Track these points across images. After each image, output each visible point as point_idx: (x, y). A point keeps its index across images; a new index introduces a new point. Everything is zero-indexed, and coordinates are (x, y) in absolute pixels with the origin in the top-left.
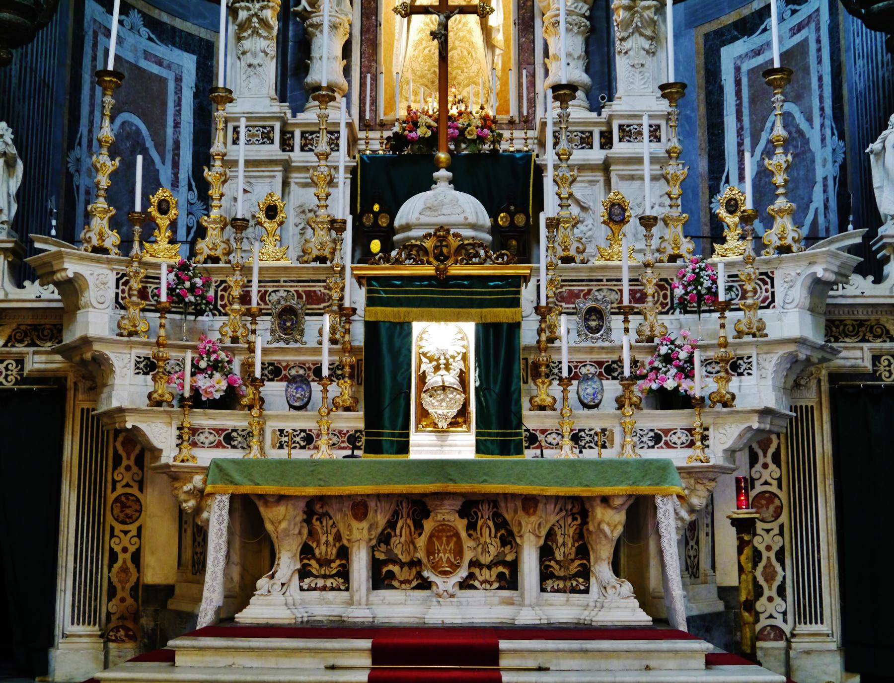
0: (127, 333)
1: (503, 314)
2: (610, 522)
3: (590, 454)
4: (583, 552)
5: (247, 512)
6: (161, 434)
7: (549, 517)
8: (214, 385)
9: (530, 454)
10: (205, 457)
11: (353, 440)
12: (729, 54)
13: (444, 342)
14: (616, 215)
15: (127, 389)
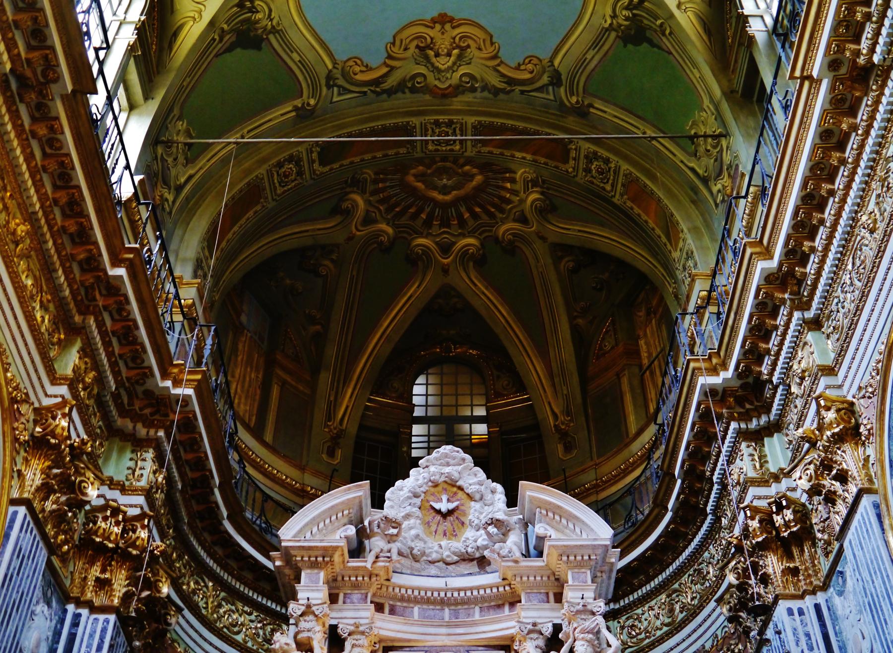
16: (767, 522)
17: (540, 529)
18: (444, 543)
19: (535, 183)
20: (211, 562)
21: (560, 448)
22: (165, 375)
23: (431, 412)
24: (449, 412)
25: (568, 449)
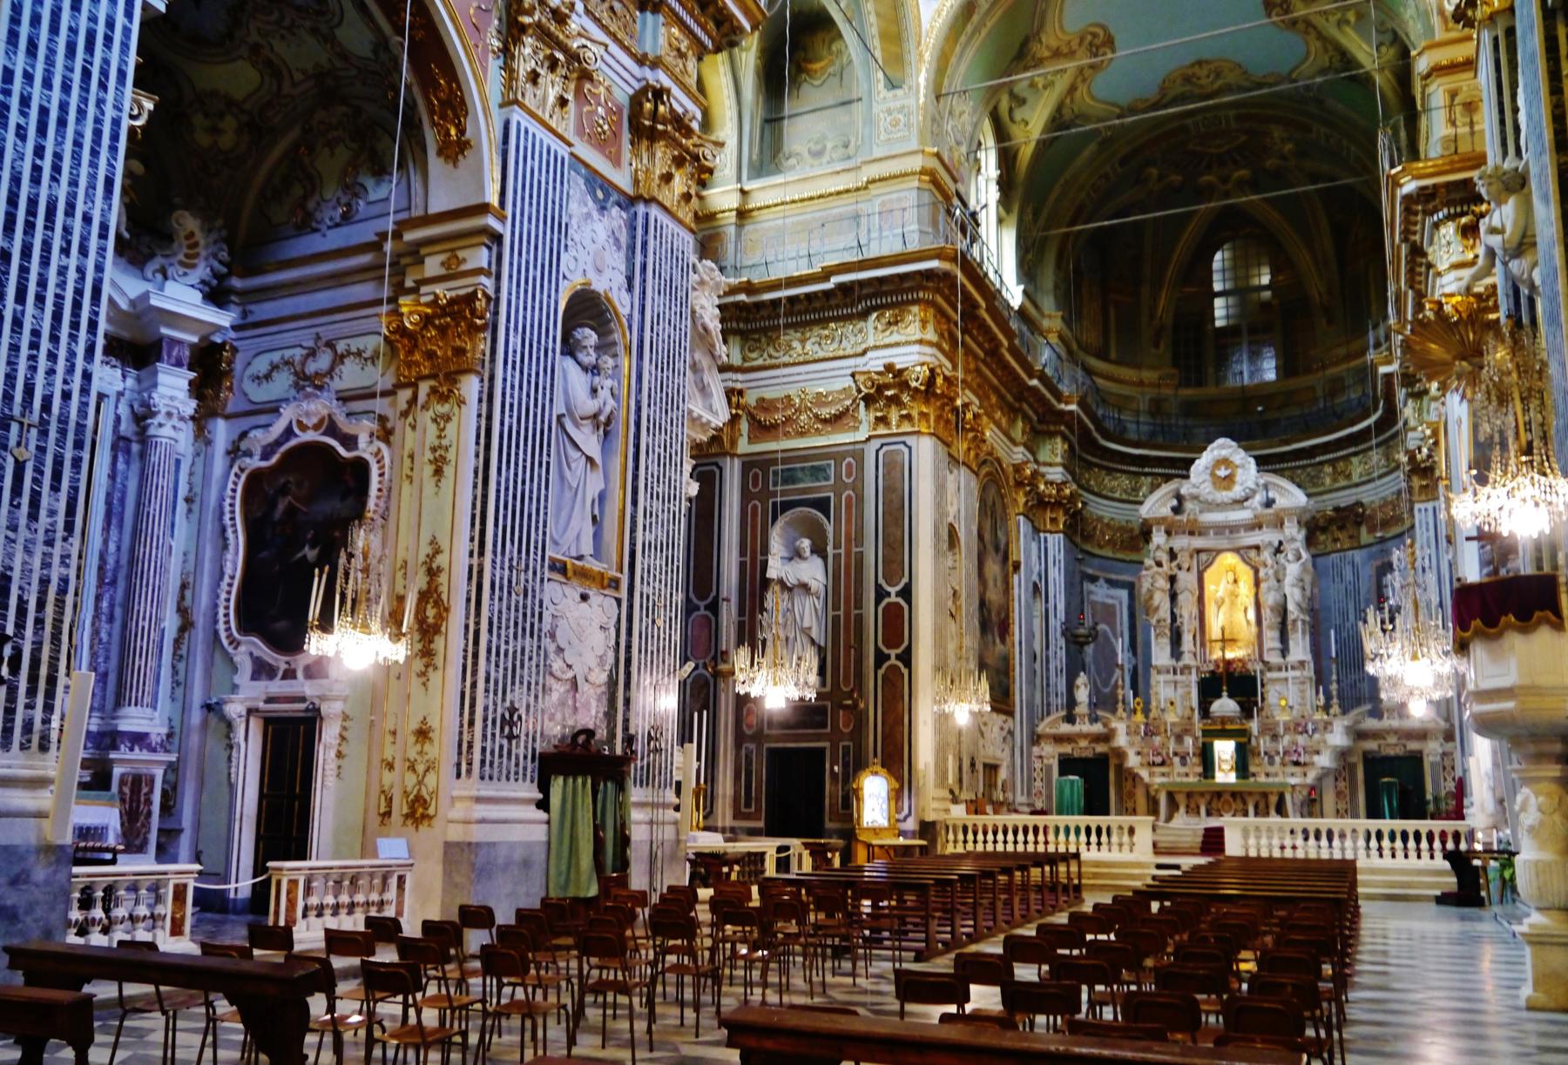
0: (1132, 744)
1: (1244, 740)
2: (1273, 800)
3: (1271, 780)
5: (1171, 796)
6: (1144, 774)
7: (1257, 798)
8: (1158, 760)
9: (1252, 779)
13: (1224, 749)
15: (1133, 761)
16: (1412, 458)
17: (1271, 495)
18: (1224, 493)
20: (1095, 460)
23: (1229, 286)
24: (1241, 284)
25: (1330, 322)
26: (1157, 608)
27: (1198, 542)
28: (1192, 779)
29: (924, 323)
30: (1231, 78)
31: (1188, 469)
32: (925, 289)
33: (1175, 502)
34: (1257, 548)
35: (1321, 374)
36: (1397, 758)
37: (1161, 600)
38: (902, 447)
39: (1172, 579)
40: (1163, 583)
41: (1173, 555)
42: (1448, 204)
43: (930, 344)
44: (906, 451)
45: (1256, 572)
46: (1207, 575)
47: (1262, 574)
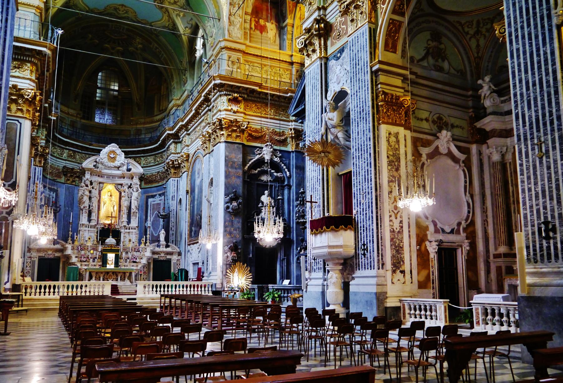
2: (128, 274)
4: (125, 277)
7: (122, 274)
8: (85, 259)
10: (86, 267)
11: (100, 265)
12: (150, 200)
13: (111, 257)
14: (130, 241)
15: (74, 260)
16: (173, 163)
19: (141, 44)
21: (137, 109)
22: (50, 115)
23: (103, 86)
25: (139, 109)
26: (84, 202)
27: (101, 180)
28: (97, 267)
29: (32, 71)
30: (130, 15)
31: (100, 153)
32: (35, 58)
33: (95, 163)
34: (121, 185)
35: (135, 126)
36: (163, 261)
37: (86, 199)
38: (16, 122)
39: (90, 192)
40: (87, 193)
41: (91, 183)
42: (226, 90)
43: (33, 81)
44: (19, 125)
45: (120, 193)
46: (102, 192)
47: (123, 194)
